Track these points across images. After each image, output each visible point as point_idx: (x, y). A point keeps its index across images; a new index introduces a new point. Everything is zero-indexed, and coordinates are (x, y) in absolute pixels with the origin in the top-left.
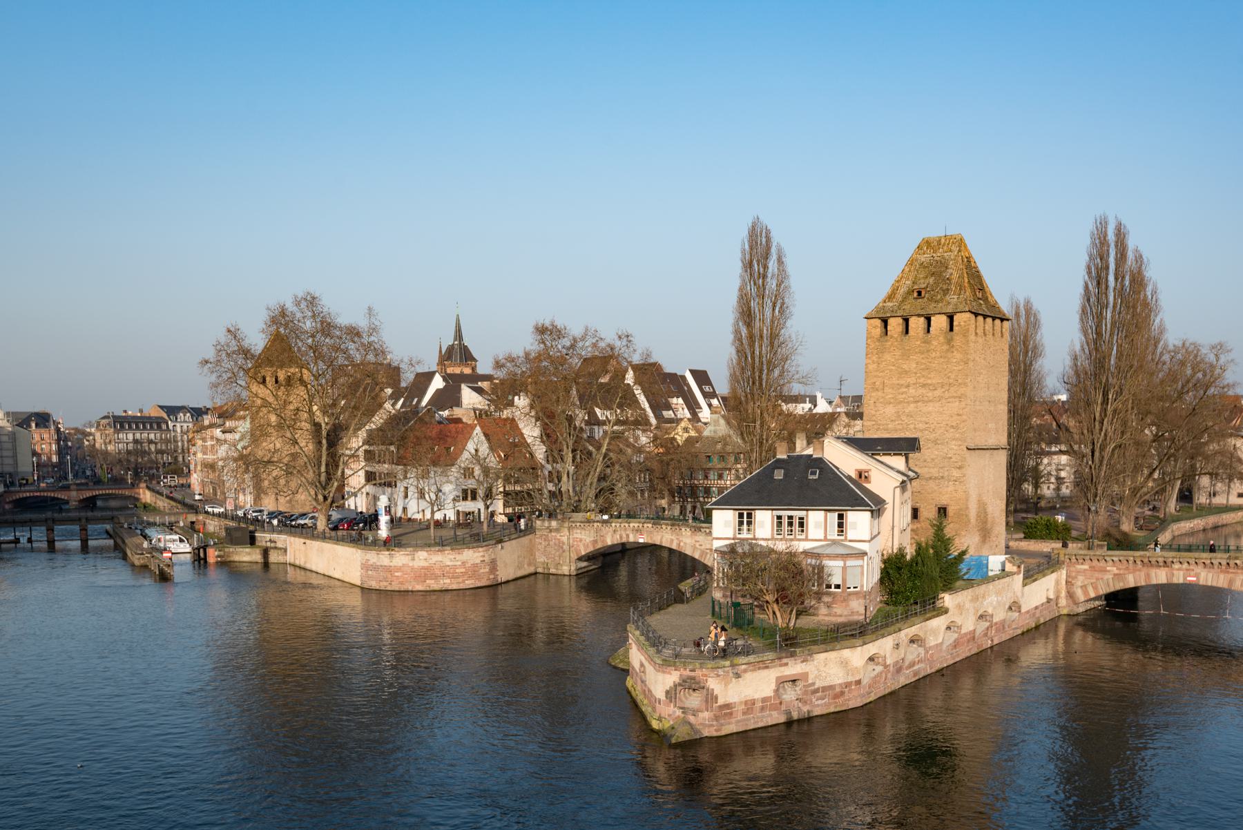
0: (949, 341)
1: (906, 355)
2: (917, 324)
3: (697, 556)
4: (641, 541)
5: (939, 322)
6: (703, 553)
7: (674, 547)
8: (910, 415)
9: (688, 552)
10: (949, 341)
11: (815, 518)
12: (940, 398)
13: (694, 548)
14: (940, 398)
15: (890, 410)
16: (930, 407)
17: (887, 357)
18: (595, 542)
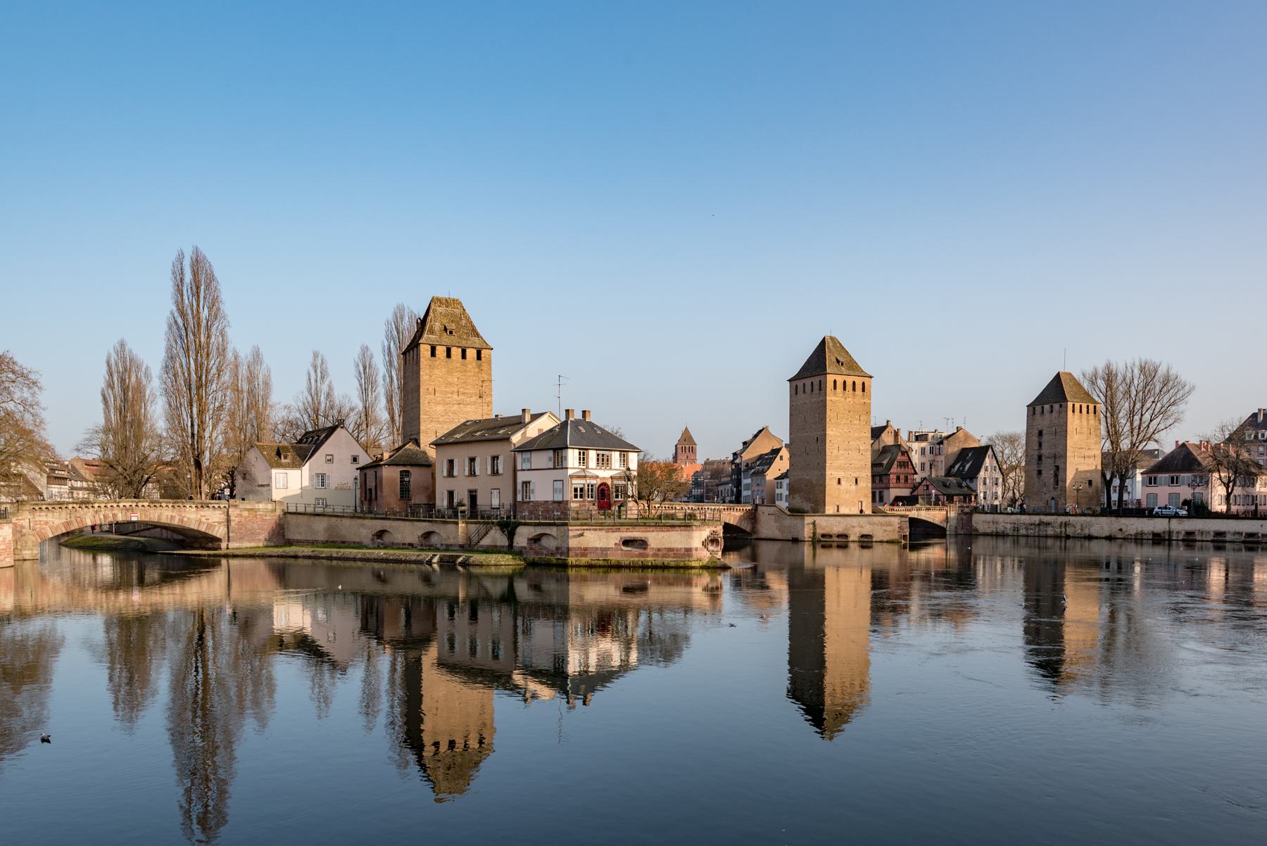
0: (479, 366)
1: (450, 372)
2: (456, 352)
3: (203, 529)
4: (134, 519)
5: (471, 353)
6: (209, 526)
7: (176, 522)
8: (454, 413)
9: (194, 526)
10: (479, 366)
11: (616, 456)
12: (475, 403)
13: (200, 522)
14: (475, 403)
15: (440, 408)
16: (468, 408)
17: (436, 371)
18: (68, 523)
